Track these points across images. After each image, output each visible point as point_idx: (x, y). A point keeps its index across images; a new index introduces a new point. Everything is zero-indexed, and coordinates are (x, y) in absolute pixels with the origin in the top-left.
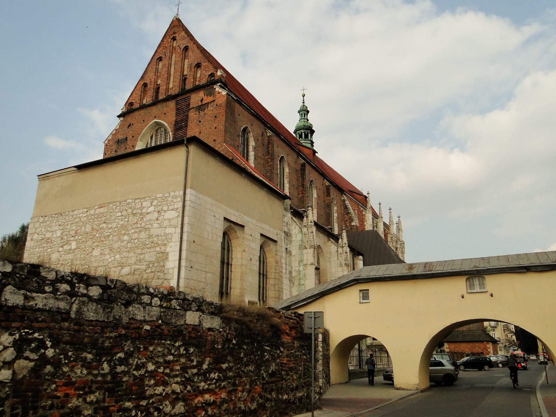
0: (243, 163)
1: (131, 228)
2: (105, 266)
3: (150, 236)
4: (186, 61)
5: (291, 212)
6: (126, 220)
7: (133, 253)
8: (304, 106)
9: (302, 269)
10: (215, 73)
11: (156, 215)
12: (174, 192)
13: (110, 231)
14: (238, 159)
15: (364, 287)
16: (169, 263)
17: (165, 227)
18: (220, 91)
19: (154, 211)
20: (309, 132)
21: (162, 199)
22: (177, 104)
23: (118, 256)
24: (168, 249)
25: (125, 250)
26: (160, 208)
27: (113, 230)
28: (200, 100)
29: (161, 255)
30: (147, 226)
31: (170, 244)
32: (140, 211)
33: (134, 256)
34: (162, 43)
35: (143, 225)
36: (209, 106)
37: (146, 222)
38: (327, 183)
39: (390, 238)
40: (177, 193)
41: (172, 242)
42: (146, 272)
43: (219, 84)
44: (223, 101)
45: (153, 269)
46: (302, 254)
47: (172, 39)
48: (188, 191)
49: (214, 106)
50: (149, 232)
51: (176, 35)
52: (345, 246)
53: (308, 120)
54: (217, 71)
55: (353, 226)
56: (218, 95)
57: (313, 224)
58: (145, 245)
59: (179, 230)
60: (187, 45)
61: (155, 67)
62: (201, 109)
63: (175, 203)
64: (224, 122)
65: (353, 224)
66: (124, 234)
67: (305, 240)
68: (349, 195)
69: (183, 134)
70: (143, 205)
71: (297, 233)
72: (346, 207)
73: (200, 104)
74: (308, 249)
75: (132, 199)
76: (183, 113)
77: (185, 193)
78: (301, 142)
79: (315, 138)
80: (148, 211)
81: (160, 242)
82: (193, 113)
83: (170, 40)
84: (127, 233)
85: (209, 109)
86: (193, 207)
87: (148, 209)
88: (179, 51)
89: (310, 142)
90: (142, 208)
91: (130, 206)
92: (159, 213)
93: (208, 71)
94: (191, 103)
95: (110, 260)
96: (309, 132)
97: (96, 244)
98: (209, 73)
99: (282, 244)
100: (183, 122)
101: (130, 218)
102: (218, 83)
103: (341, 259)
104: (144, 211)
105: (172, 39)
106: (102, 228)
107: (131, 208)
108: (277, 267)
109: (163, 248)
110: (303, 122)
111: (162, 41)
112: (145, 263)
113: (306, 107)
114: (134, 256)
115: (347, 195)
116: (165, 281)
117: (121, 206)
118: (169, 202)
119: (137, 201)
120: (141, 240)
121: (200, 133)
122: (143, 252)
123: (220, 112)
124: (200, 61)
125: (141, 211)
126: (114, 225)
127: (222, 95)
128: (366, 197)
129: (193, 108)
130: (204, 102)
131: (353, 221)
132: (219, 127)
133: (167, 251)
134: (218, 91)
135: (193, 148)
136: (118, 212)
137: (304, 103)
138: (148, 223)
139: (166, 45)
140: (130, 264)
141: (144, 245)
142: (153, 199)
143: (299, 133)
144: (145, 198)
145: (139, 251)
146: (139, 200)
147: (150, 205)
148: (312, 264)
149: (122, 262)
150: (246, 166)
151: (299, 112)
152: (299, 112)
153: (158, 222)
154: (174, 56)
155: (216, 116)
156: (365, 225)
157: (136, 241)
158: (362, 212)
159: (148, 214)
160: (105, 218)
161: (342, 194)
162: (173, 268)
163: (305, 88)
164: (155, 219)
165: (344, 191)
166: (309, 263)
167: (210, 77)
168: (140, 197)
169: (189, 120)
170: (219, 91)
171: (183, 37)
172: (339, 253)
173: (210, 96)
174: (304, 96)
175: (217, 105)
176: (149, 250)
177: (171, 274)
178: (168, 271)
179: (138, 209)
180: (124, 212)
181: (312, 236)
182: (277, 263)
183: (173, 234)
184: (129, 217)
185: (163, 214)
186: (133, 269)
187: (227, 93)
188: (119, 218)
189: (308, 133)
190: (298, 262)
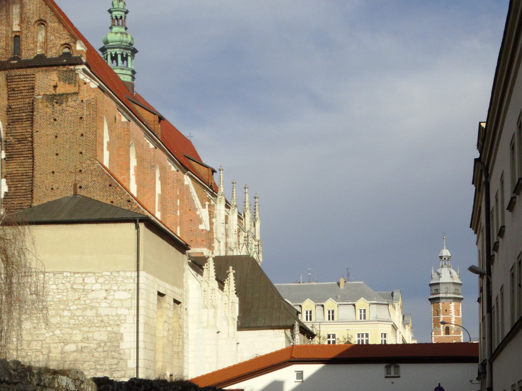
0: (127, 193)
1: (72, 303)
2: (41, 341)
3: (98, 315)
5: (189, 263)
6: (64, 294)
7: (78, 330)
10: (72, 44)
11: (104, 294)
12: (125, 272)
14: (118, 186)
17: (117, 308)
18: (88, 81)
19: (101, 289)
20: (129, 52)
21: (111, 278)
22: (9, 79)
23: (57, 332)
24: (122, 330)
25: (67, 326)
26: (107, 287)
29: (114, 335)
30: (93, 304)
31: (124, 325)
32: (82, 287)
33: (80, 334)
36: (69, 99)
37: (91, 300)
39: (244, 239)
41: (126, 323)
42: (97, 350)
45: (105, 349)
48: (141, 273)
49: (78, 102)
50: (97, 310)
54: (75, 43)
56: (84, 87)
58: (93, 323)
62: (55, 101)
63: (126, 284)
65: (201, 227)
66: (63, 310)
69: (25, 131)
70: (85, 281)
73: (53, 92)
75: (70, 273)
76: (21, 98)
78: (117, 71)
80: (93, 289)
81: (111, 322)
84: (67, 308)
85: (70, 103)
86: (146, 290)
89: (130, 73)
90: (84, 283)
91: (68, 280)
92: (107, 292)
93: (60, 38)
94: (36, 87)
95: (47, 335)
96: (129, 54)
100: (24, 112)
101: (69, 293)
107: (69, 282)
108: (181, 333)
110: (119, 35)
114: (80, 334)
116: (121, 361)
117: (56, 278)
119: (77, 275)
120: (86, 318)
121: (56, 137)
122: (91, 330)
125: (84, 287)
127: (91, 88)
130: (60, 90)
131: (201, 223)
133: (121, 331)
135: (142, 226)
136: (52, 284)
138: (94, 301)
140: (76, 342)
142: (99, 277)
143: (111, 53)
144: (87, 273)
145: (86, 329)
146: (79, 275)
147: (94, 282)
149: (64, 338)
150: (132, 198)
157: (80, 318)
159: (93, 291)
162: (129, 349)
164: (103, 298)
168: (80, 271)
170: (85, 80)
173: (69, 83)
175: (82, 101)
176: (98, 329)
177: (128, 354)
178: (124, 351)
179: (79, 284)
180: (61, 285)
182: (181, 328)
183: (127, 316)
184: (68, 291)
185: (113, 294)
189: (127, 55)
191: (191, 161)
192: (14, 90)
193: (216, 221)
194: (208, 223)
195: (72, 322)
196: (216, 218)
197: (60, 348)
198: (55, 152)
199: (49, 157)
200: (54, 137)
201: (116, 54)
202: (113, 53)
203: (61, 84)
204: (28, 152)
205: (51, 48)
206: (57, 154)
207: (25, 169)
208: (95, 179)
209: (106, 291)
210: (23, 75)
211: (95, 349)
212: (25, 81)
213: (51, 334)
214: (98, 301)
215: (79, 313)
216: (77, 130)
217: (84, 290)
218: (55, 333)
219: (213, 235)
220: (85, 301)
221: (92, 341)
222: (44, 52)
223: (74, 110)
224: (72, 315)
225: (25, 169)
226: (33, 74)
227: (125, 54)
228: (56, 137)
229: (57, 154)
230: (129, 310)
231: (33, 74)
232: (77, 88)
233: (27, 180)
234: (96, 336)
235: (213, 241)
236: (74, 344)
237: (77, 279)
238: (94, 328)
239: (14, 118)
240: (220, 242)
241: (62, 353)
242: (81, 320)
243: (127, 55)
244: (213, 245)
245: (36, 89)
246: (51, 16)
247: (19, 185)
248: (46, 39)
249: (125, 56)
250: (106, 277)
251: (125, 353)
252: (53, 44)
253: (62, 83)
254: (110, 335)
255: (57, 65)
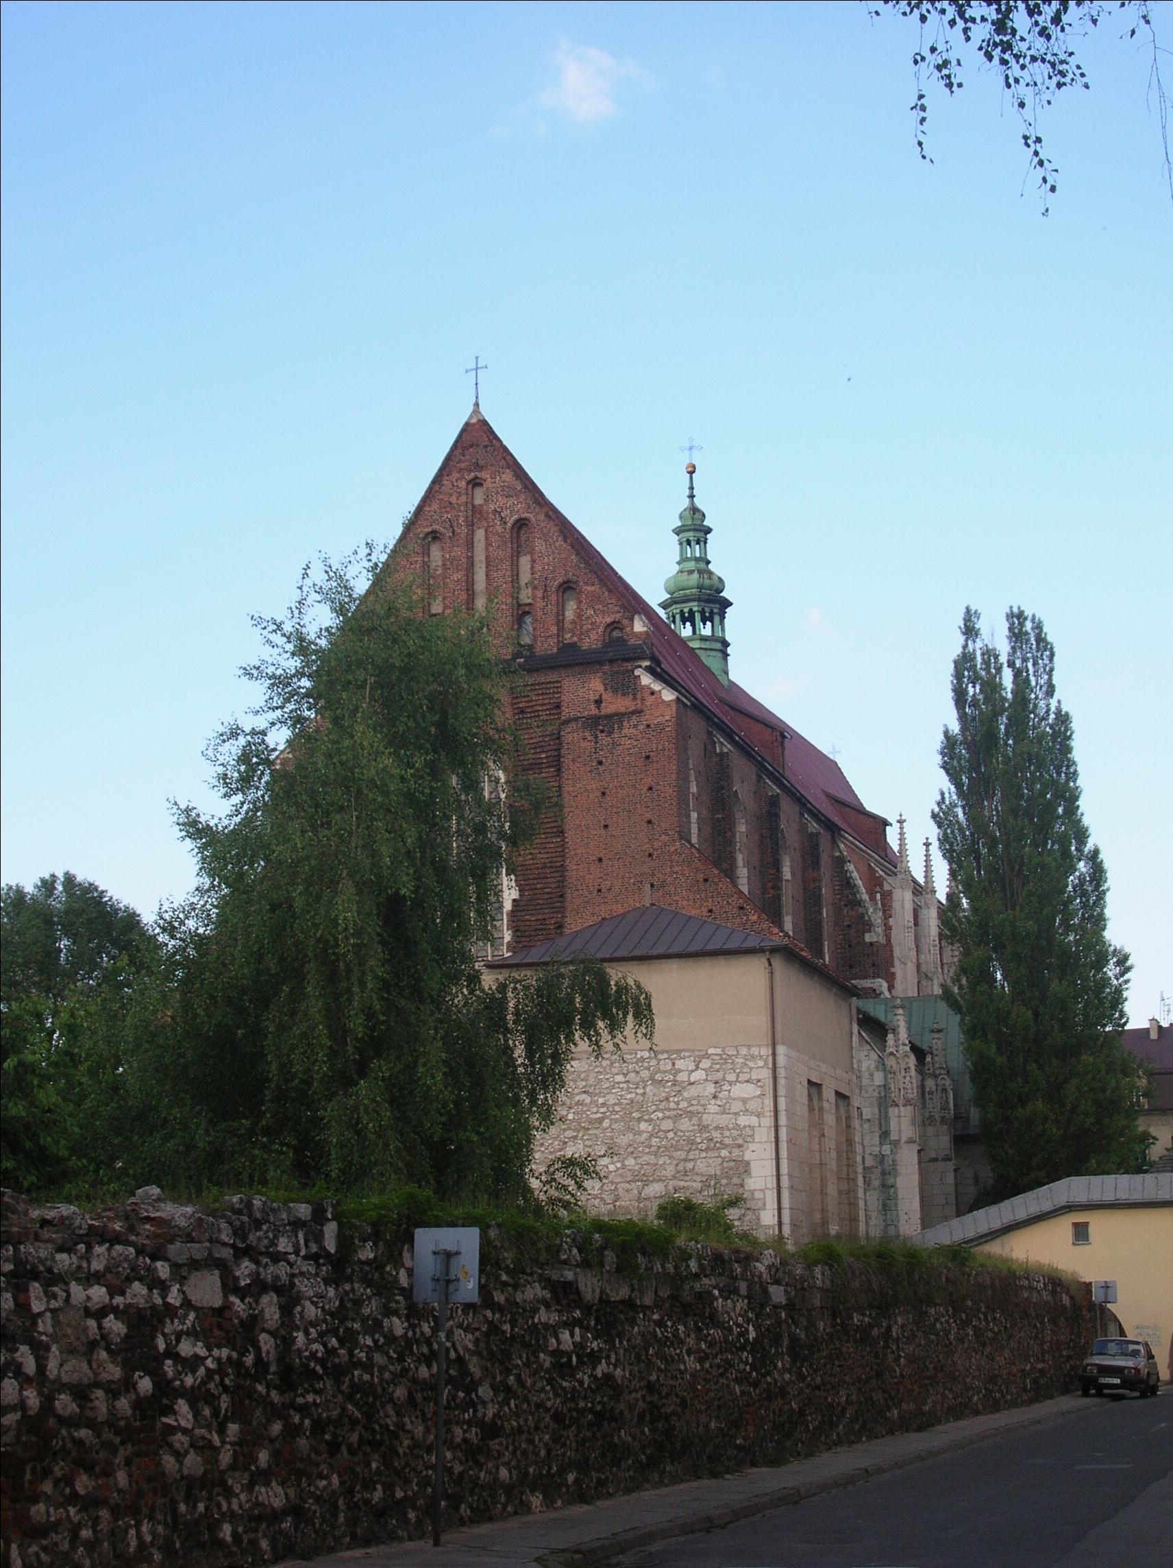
3: (703, 1128)
4: (525, 561)
6: (640, 1091)
8: (694, 510)
9: (888, 1152)
10: (625, 622)
11: (711, 1088)
12: (749, 1047)
13: (602, 1110)
15: (1080, 1218)
16: (753, 1179)
19: (706, 1080)
23: (630, 1162)
25: (647, 1150)
26: (719, 1075)
27: (611, 1109)
28: (592, 698)
30: (691, 1108)
31: (752, 1147)
34: (437, 488)
35: (683, 1105)
37: (689, 1100)
38: (814, 826)
40: (755, 1051)
41: (754, 1142)
43: (647, 663)
44: (667, 718)
46: (884, 1120)
47: (468, 483)
48: (781, 1049)
49: (641, 727)
50: (700, 1119)
51: (484, 475)
52: (940, 1074)
53: (708, 562)
54: (632, 620)
55: (871, 944)
56: (650, 700)
57: (908, 1048)
59: (768, 1121)
60: (523, 516)
61: (420, 559)
63: (751, 1069)
64: (674, 776)
65: (868, 938)
66: (639, 1120)
67: (892, 1085)
68: (851, 838)
71: (873, 1067)
72: (848, 882)
73: (594, 711)
74: (902, 1109)
77: (774, 1054)
79: (734, 625)
80: (692, 1080)
81: (727, 1141)
82: (575, 735)
83: (463, 484)
84: (646, 1117)
87: (690, 1074)
88: (499, 529)
93: (603, 612)
95: (612, 1168)
96: (715, 611)
97: (569, 1133)
98: (609, 620)
99: (856, 1102)
100: (543, 752)
102: (643, 659)
103: (931, 1105)
104: (682, 1077)
105: (468, 483)
106: (578, 1103)
107: (648, 1069)
109: (736, 1152)
110: (696, 575)
111: (437, 480)
112: (699, 1178)
113: (704, 515)
114: (670, 1164)
115: (846, 839)
116: (749, 1212)
118: (738, 1066)
119: (661, 1056)
121: (604, 794)
122: (691, 1157)
123: (660, 747)
124: (573, 575)
126: (612, 1099)
127: (663, 702)
128: (885, 823)
129: (576, 719)
132: (659, 787)
134: (648, 687)
135: (777, 963)
137: (692, 496)
139: (453, 499)
141: (692, 1144)
143: (682, 613)
144: (678, 1052)
146: (666, 1056)
147: (692, 1067)
148: (910, 1141)
151: (677, 532)
152: (677, 532)
153: (719, 1102)
154: (480, 534)
155: (648, 757)
157: (671, 1135)
159: (693, 1084)
160: (584, 1083)
161: (834, 841)
163: (695, 443)
165: (840, 829)
166: (904, 1139)
167: (609, 630)
169: (563, 752)
170: (652, 686)
171: (509, 487)
172: (927, 1090)
174: (691, 473)
175: (648, 726)
176: (704, 1154)
179: (666, 1072)
180: (633, 1075)
181: (908, 1078)
182: (851, 1145)
186: (670, 1187)
187: (678, 698)
188: (621, 1086)
189: (712, 613)
190: (877, 1135)
192: (523, 712)
194: (880, 930)
195: (655, 1141)
197: (635, 1192)
198: (603, 823)
199: (593, 832)
200: (598, 794)
201: (691, 612)
202: (686, 610)
203: (607, 697)
204: (552, 825)
205: (588, 630)
206: (606, 826)
207: (549, 855)
208: (676, 869)
209: (716, 1083)
210: (539, 684)
211: (700, 1192)
212: (543, 694)
213: (619, 1165)
214: (702, 1102)
215: (666, 1125)
216: (641, 779)
217: (675, 1083)
218: (627, 1163)
220: (678, 1103)
221: (694, 1178)
222: (575, 639)
223: (635, 743)
224: (654, 1129)
225: (549, 855)
226: (557, 682)
227: (707, 610)
228: (604, 794)
229: (606, 826)
230: (758, 1116)
231: (557, 682)
232: (639, 702)
233: (553, 875)
234: (701, 1166)
236: (660, 1184)
237: (662, 1062)
238: (697, 1152)
239: (526, 763)
241: (639, 1200)
242: (672, 1138)
243: (712, 613)
244: (893, 970)
245: (563, 708)
246: (585, 574)
247: (539, 886)
248: (579, 616)
250: (716, 1057)
251: (753, 1199)
252: (592, 624)
253: (610, 695)
254: (725, 1165)
255: (600, 663)
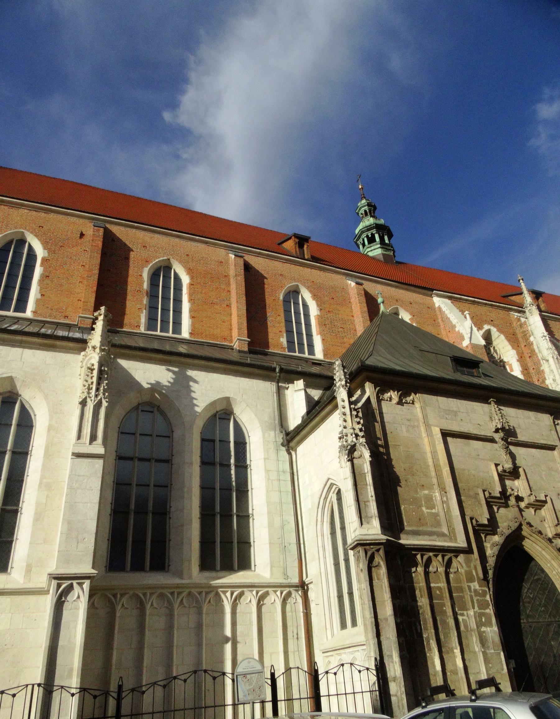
96: (374, 232)
156: (532, 344)
158: (519, 320)
191: (510, 298)
193: (535, 338)
196: (533, 335)
219: (537, 357)
235: (540, 363)
240: (547, 361)
244: (542, 369)
249: (370, 236)
